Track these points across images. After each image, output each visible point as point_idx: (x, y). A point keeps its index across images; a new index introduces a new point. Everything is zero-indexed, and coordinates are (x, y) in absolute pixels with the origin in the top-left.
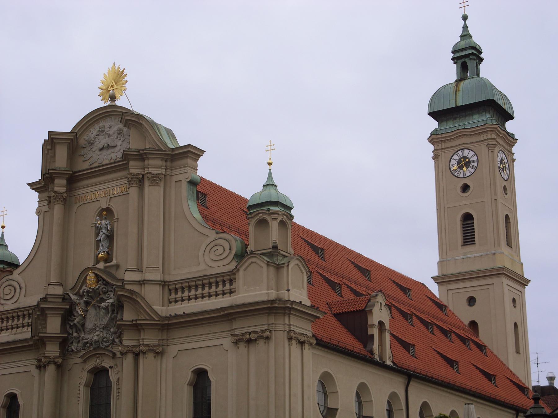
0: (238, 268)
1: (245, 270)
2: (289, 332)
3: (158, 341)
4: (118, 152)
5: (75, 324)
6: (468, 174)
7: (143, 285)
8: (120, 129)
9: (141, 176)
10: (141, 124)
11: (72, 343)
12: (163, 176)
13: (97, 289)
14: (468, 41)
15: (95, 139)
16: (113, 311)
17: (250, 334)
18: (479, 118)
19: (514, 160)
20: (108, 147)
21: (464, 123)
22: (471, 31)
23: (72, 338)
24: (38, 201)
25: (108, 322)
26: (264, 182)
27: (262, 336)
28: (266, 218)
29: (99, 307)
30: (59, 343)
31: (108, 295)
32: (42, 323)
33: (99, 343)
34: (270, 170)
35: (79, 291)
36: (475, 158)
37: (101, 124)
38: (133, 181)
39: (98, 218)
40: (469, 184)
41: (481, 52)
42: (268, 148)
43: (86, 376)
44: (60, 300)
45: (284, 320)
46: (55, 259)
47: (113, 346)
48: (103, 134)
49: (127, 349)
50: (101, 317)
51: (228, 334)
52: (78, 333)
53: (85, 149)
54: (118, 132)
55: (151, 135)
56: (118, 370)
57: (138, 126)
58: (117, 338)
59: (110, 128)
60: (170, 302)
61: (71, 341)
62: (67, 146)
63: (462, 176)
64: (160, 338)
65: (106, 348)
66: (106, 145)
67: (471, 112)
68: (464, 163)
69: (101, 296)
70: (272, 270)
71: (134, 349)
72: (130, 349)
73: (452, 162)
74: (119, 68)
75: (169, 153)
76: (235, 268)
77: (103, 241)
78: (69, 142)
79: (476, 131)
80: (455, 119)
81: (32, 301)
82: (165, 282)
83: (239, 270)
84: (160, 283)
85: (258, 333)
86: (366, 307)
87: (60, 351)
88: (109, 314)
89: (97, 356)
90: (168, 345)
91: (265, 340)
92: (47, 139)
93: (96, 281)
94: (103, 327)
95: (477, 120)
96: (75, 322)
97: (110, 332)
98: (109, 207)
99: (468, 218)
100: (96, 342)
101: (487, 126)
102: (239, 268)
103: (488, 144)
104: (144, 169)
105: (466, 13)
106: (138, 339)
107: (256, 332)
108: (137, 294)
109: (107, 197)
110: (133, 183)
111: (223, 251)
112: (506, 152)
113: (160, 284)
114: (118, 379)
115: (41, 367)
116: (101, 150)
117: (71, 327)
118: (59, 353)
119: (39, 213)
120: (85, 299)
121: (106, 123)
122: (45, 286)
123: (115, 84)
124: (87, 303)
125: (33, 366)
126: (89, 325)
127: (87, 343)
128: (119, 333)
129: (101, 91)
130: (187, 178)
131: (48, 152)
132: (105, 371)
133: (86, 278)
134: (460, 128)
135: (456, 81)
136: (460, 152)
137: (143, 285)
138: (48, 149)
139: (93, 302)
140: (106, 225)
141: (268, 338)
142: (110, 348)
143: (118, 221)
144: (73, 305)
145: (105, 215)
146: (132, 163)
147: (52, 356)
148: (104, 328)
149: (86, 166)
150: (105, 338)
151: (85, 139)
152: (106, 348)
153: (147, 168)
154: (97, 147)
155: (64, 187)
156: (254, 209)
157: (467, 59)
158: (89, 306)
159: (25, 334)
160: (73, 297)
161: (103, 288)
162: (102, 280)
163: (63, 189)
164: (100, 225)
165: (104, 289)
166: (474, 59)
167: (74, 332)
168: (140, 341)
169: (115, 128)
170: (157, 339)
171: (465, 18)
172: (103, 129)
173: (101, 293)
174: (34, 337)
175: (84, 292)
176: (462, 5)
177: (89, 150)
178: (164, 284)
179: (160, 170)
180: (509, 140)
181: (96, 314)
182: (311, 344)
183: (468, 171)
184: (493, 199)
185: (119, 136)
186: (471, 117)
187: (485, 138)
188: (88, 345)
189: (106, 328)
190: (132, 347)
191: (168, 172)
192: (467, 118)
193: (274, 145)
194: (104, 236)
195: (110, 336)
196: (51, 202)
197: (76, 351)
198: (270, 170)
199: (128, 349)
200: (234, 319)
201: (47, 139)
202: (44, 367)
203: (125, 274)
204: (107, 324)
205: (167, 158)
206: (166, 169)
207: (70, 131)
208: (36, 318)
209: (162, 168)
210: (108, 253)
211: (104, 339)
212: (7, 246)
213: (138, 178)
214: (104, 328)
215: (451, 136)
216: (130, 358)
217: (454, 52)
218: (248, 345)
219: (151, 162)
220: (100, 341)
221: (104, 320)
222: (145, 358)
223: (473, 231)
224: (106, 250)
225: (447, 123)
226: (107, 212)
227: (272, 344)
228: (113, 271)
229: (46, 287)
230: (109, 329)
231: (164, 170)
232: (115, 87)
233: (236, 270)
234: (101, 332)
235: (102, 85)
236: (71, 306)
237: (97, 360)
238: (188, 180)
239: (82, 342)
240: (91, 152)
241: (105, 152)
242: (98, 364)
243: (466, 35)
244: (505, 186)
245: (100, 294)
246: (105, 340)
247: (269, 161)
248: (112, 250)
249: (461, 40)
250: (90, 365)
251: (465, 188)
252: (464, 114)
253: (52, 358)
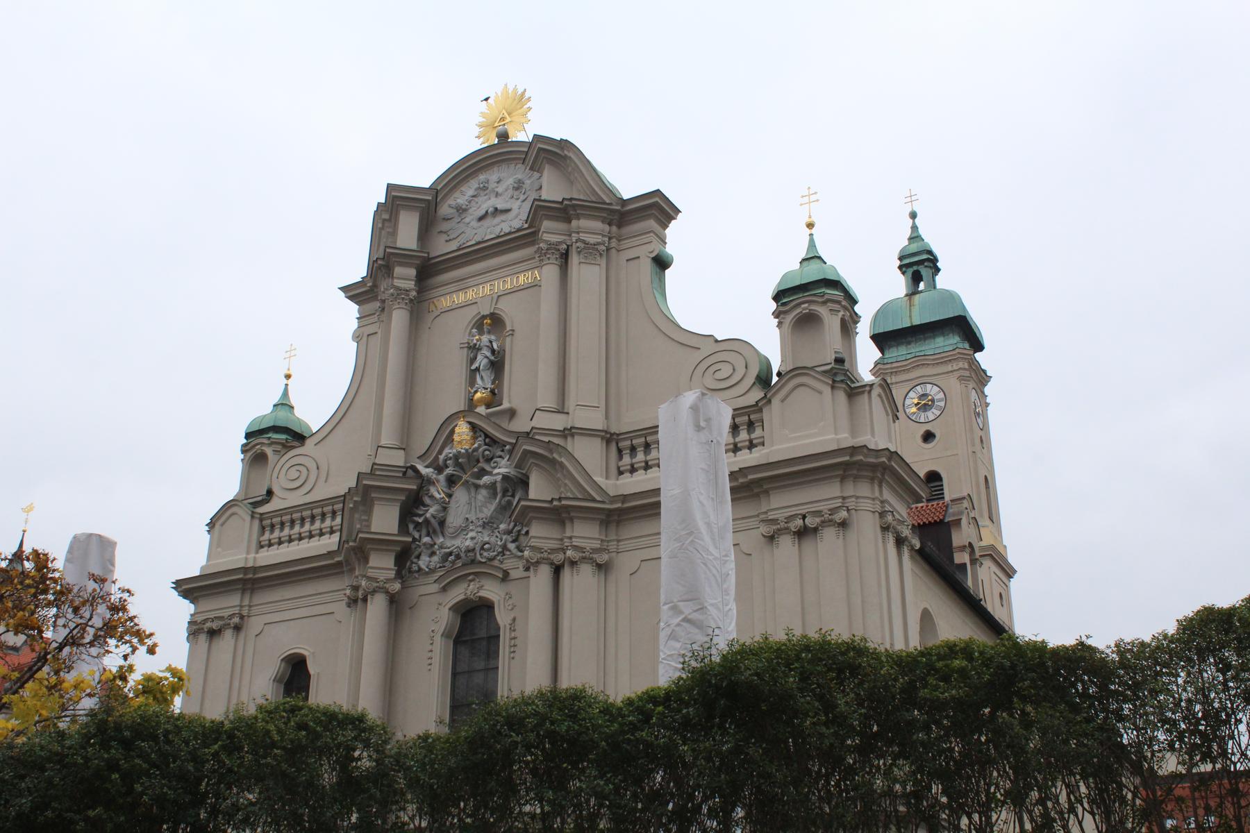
0: (768, 396)
1: (783, 401)
2: (882, 514)
3: (599, 542)
4: (514, 219)
5: (427, 521)
6: (931, 417)
7: (569, 439)
8: (520, 180)
9: (565, 246)
10: (565, 158)
11: (418, 557)
12: (605, 248)
13: (476, 450)
14: (920, 243)
15: (470, 202)
16: (505, 492)
17: (804, 517)
18: (944, 341)
19: (987, 405)
20: (494, 214)
21: (923, 348)
22: (921, 232)
23: (419, 546)
24: (357, 318)
25: (493, 513)
26: (803, 255)
27: (831, 521)
28: (817, 311)
29: (477, 487)
30: (394, 554)
31: (496, 464)
32: (363, 517)
33: (475, 554)
34: (811, 235)
35: (436, 458)
36: (941, 395)
37: (482, 177)
38: (549, 254)
39: (474, 330)
40: (933, 431)
41: (937, 261)
42: (806, 199)
43: (447, 616)
44: (401, 475)
45: (873, 492)
46: (391, 406)
47: (504, 557)
48: (486, 192)
49: (539, 556)
50: (480, 504)
51: (753, 523)
52: (431, 537)
53: (451, 221)
54: (516, 185)
55: (583, 174)
56: (513, 604)
57: (559, 163)
58: (513, 541)
59: (498, 182)
60: (621, 473)
61: (416, 553)
62: (418, 214)
63: (922, 420)
64: (604, 538)
65: (488, 563)
66: (491, 210)
67: (932, 334)
69: (480, 465)
70: (841, 396)
71: (552, 557)
72: (545, 555)
73: (908, 402)
74: (515, 89)
75: (618, 208)
76: (763, 398)
77: (482, 370)
78: (424, 205)
79: (942, 358)
80: (909, 343)
81: (342, 483)
82: (612, 435)
83: (769, 401)
84: (603, 434)
85: (823, 516)
86: (944, 516)
87: (396, 568)
88: (495, 498)
89: (471, 577)
90: (620, 551)
91: (837, 529)
92: (384, 202)
93: (472, 437)
94: (484, 522)
95: (941, 344)
96: (428, 515)
97: (499, 532)
98: (496, 311)
100: (469, 550)
101: (957, 351)
102: (771, 396)
103: (961, 376)
104: (570, 235)
105: (914, 209)
106: (560, 537)
107: (818, 513)
108: (560, 450)
109: (493, 295)
110: (549, 258)
111: (732, 371)
112: (978, 391)
113: (603, 438)
114: (514, 619)
115: (357, 601)
116: (481, 219)
117: (417, 525)
118: (394, 572)
119: (358, 337)
120: (448, 471)
121: (492, 176)
122: (370, 453)
123: (507, 116)
124: (451, 481)
125: (341, 602)
126: (454, 520)
127: (450, 554)
128: (517, 534)
129: (481, 129)
130: (652, 252)
131: (383, 224)
132: (486, 607)
133: (452, 432)
134: (918, 354)
135: (906, 295)
136: (918, 388)
137: (569, 439)
138: (384, 220)
139: (465, 477)
140: (491, 342)
141: (843, 524)
142: (496, 563)
143: (512, 335)
144: (425, 482)
145: (490, 325)
146: (547, 224)
147: (382, 578)
148: (484, 526)
149: (453, 246)
150: (488, 543)
151: (450, 206)
152: (488, 563)
153: (575, 232)
154: (472, 217)
155: (412, 280)
156: (790, 296)
157: (921, 267)
158: (454, 487)
159: (330, 542)
160: (424, 471)
161: (486, 450)
162: (483, 436)
163: (411, 285)
164: (478, 343)
165: (487, 453)
166: (930, 267)
167: (423, 535)
168: (565, 540)
169: (511, 181)
170: (598, 539)
171: (913, 215)
172: (486, 185)
173: (481, 460)
174: (347, 542)
175: (445, 460)
176: (909, 199)
177: (459, 222)
178: (609, 438)
179: (600, 237)
180: (982, 376)
181: (470, 499)
182: (912, 548)
183: (931, 415)
184: (970, 451)
185: (516, 193)
186: (933, 340)
187: (955, 368)
188: (451, 558)
189: (488, 524)
190: (549, 553)
191: (614, 243)
192: (927, 342)
193: (816, 193)
194: (485, 361)
195: (498, 539)
196: (386, 309)
197: (427, 570)
198: (811, 235)
199: (542, 555)
200: (767, 492)
201: (384, 202)
202: (365, 600)
203: (531, 420)
204: (491, 517)
205: (612, 220)
206: (610, 238)
207: (428, 187)
208: (351, 508)
209: (603, 236)
210: (492, 392)
211: (484, 545)
212: (293, 408)
213: (559, 250)
214: (484, 526)
215: (906, 365)
216: (545, 572)
217: (900, 259)
218: (799, 541)
219: (584, 223)
220: (478, 549)
221: (485, 510)
222: (575, 573)
223: (942, 496)
224: (489, 386)
225: (897, 348)
226: (494, 322)
227: (852, 535)
228: (505, 425)
229: (370, 455)
230: (495, 526)
231: (607, 239)
232: (508, 119)
233: (764, 401)
234: (480, 532)
235: (484, 120)
236: (421, 488)
237: (469, 586)
238: (653, 255)
239: (440, 553)
240: (461, 225)
241: (487, 222)
242: (472, 592)
243: (915, 237)
244: (981, 437)
245: (478, 461)
246: (486, 546)
247: (809, 220)
248: (500, 386)
249: (909, 244)
250: (458, 594)
251: (928, 437)
252: (922, 336)
253: (382, 581)
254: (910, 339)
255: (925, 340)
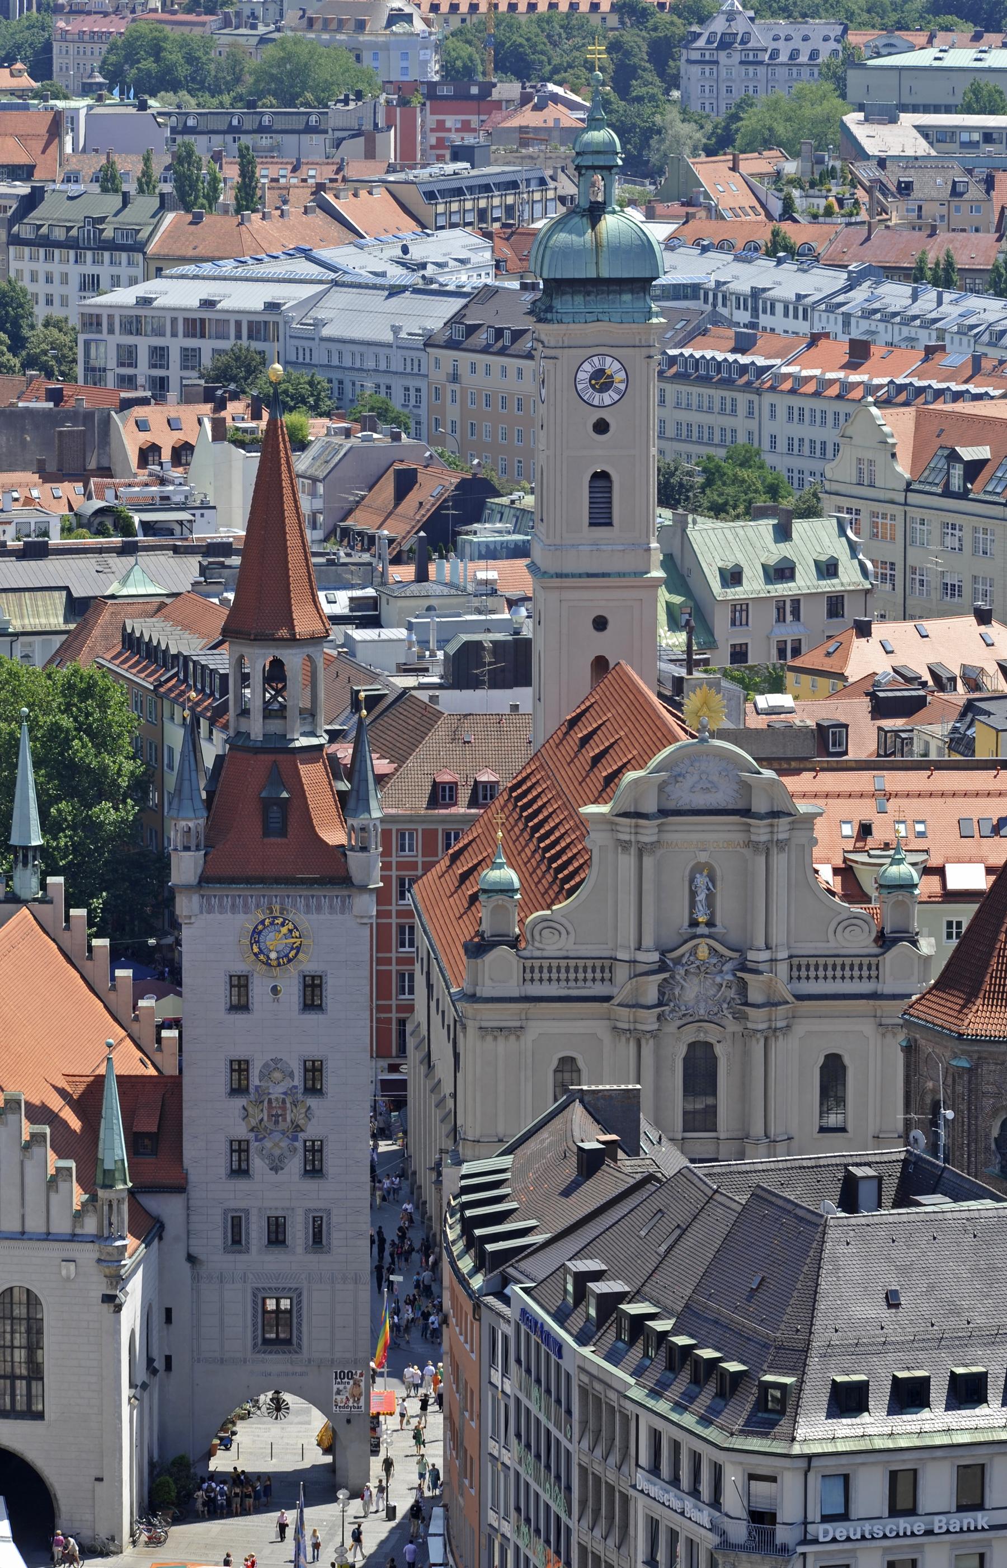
6: (607, 401)
36: (622, 375)
63: (596, 403)
68: (601, 381)
73: (581, 375)
80: (588, 294)
99: (601, 478)
136: (595, 359)
183: (607, 398)
251: (601, 427)
254: (590, 288)
255: (608, 294)
